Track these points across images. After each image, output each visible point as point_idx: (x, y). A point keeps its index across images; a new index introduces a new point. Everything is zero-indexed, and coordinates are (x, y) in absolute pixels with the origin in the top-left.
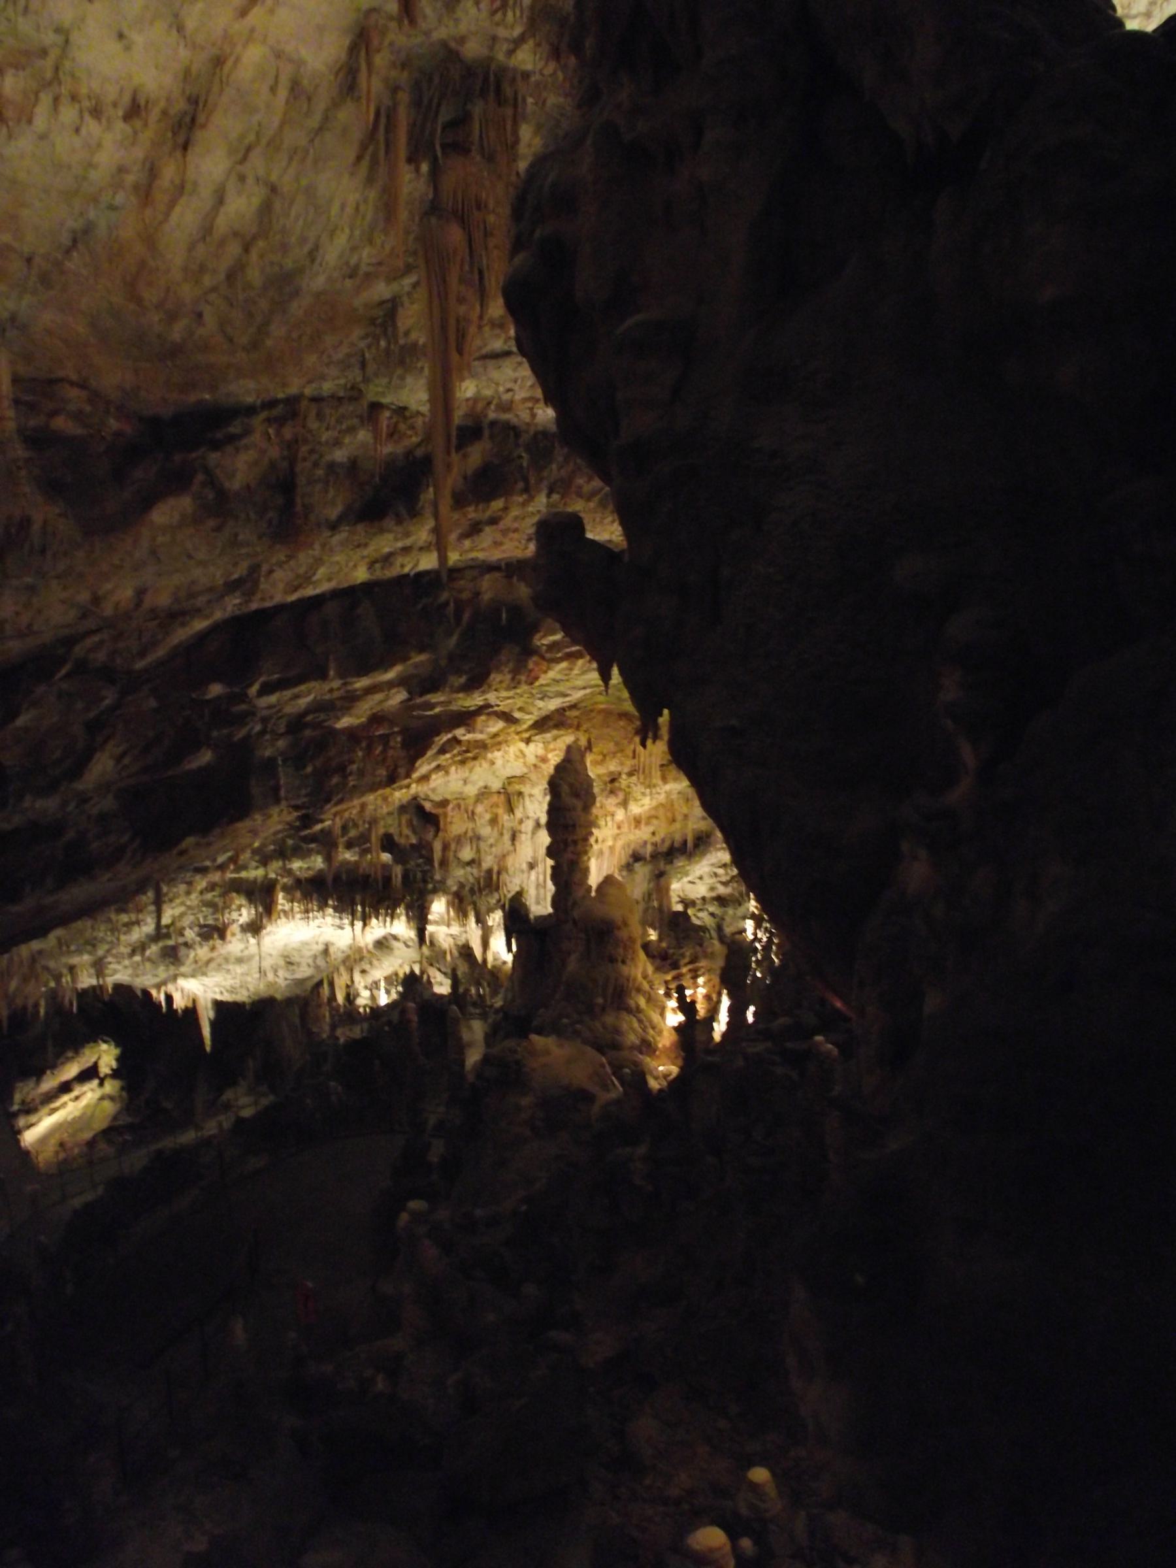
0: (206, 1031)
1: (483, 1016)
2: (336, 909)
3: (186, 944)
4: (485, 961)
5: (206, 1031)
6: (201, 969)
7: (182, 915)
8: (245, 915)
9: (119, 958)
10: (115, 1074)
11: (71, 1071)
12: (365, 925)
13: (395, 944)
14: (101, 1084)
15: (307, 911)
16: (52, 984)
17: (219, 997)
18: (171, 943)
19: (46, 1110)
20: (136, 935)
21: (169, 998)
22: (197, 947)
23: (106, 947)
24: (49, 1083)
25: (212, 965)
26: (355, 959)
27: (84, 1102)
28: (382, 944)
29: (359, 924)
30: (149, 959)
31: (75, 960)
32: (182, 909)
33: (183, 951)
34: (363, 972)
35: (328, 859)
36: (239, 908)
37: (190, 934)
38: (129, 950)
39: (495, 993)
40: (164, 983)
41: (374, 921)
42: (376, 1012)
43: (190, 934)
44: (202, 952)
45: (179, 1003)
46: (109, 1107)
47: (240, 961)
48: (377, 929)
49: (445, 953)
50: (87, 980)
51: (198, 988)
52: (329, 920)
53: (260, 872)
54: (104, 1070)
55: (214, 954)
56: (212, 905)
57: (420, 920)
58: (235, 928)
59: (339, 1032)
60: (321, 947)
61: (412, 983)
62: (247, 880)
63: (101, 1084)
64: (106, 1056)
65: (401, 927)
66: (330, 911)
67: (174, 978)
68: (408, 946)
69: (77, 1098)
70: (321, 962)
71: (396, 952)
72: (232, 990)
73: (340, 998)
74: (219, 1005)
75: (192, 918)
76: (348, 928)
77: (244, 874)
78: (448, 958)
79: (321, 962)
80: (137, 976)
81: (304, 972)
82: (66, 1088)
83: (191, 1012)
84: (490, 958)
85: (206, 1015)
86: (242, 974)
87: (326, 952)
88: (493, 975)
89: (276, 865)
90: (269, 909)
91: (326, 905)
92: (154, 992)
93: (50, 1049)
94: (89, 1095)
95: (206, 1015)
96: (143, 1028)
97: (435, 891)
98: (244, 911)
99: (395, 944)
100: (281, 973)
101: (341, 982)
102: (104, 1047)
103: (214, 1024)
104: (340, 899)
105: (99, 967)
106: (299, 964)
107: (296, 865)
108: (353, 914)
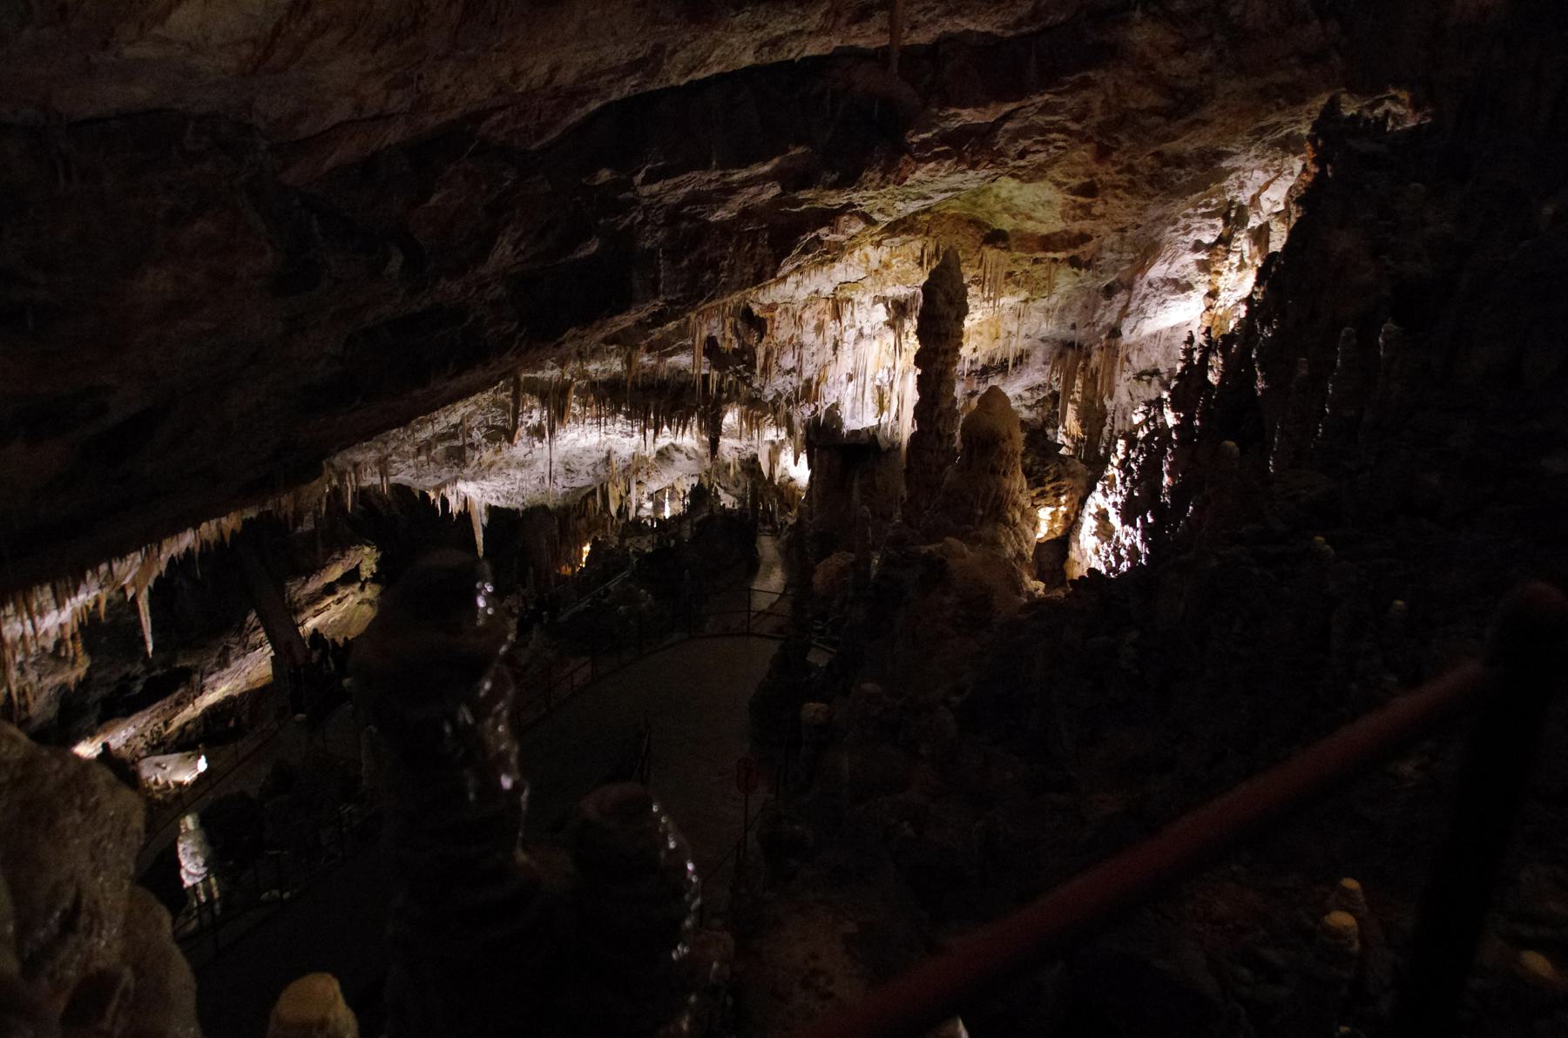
0: (479, 537)
1: (775, 533)
2: (628, 416)
3: (471, 445)
4: (772, 476)
5: (479, 537)
6: (480, 474)
7: (471, 415)
8: (535, 417)
9: (404, 456)
10: (375, 579)
11: (336, 572)
12: (656, 433)
13: (676, 455)
15: (599, 417)
16: (335, 482)
17: (494, 503)
18: (458, 443)
19: (311, 611)
20: (426, 434)
21: (445, 502)
22: (483, 449)
23: (394, 445)
24: (314, 585)
25: (494, 469)
26: (636, 468)
27: (345, 604)
28: (663, 455)
29: (650, 432)
30: (433, 460)
31: (359, 457)
32: (471, 409)
33: (469, 452)
34: (639, 483)
35: (629, 361)
36: (531, 409)
37: (477, 435)
38: (413, 449)
39: (782, 512)
40: (443, 485)
41: (666, 428)
43: (477, 435)
44: (487, 455)
45: (455, 506)
46: (368, 612)
47: (521, 465)
48: (666, 438)
49: (728, 466)
50: (371, 479)
51: (475, 493)
52: (618, 426)
53: (556, 373)
54: (365, 573)
55: (498, 458)
56: (504, 406)
57: (714, 431)
58: (522, 431)
59: (627, 542)
60: (604, 455)
61: (700, 495)
62: (541, 381)
63: (362, 589)
64: (366, 559)
65: (690, 439)
66: (621, 416)
67: (455, 480)
68: (690, 458)
69: (339, 601)
70: (601, 471)
71: (677, 464)
73: (613, 509)
74: (492, 511)
75: (480, 418)
76: (637, 437)
77: (539, 374)
78: (732, 472)
79: (601, 471)
80: (419, 477)
81: (582, 481)
82: (330, 589)
83: (465, 516)
84: (778, 473)
85: (480, 521)
86: (522, 480)
87: (607, 460)
88: (784, 491)
89: (573, 366)
90: (559, 414)
91: (620, 411)
92: (432, 495)
93: (320, 549)
94: (351, 598)
95: (480, 521)
96: (412, 532)
97: (729, 401)
98: (536, 414)
99: (676, 455)
100: (560, 481)
101: (614, 493)
102: (367, 550)
103: (485, 530)
104: (634, 406)
105: (383, 466)
106: (578, 472)
107: (593, 367)
108: (646, 419)
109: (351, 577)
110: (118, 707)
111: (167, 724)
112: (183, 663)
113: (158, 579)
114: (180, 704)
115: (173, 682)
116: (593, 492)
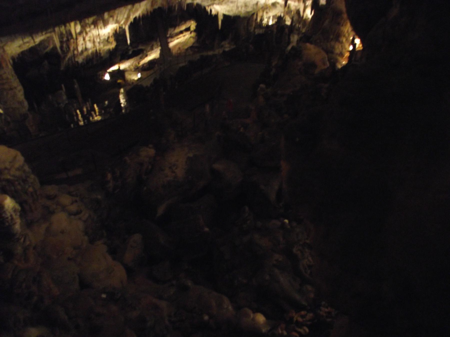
10: (195, 31)
11: (183, 28)
14: (191, 33)
21: (211, 11)
24: (177, 30)
34: (267, 13)
42: (268, 26)
45: (214, 13)
46: (192, 40)
61: (280, 19)
63: (191, 33)
64: (193, 25)
67: (213, 4)
69: (184, 36)
70: (255, 7)
72: (229, 11)
73: (259, 20)
74: (225, 16)
78: (293, 13)
79: (255, 7)
81: (249, 9)
82: (181, 32)
85: (220, 18)
87: (257, 4)
92: (207, 8)
95: (220, 18)
101: (260, 14)
103: (223, 21)
109: (188, 29)
110: (125, 57)
111: (139, 63)
112: (140, 47)
113: (131, 24)
114: (142, 58)
115: (139, 53)
116: (253, 14)
